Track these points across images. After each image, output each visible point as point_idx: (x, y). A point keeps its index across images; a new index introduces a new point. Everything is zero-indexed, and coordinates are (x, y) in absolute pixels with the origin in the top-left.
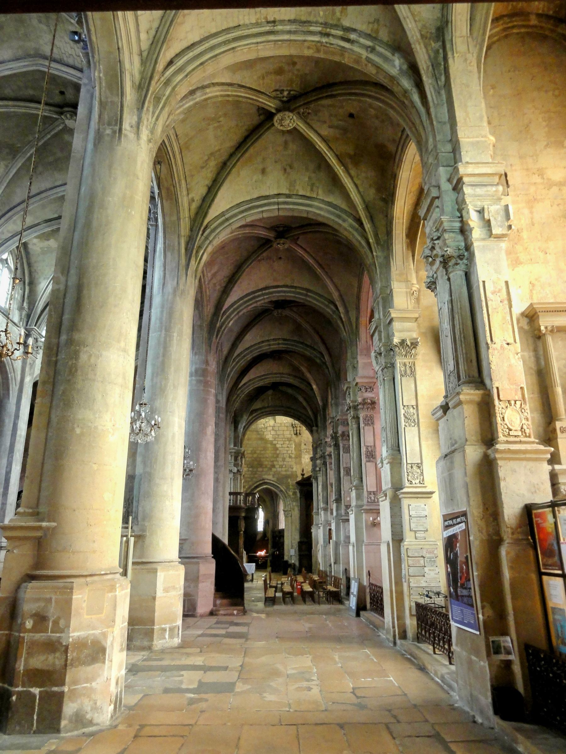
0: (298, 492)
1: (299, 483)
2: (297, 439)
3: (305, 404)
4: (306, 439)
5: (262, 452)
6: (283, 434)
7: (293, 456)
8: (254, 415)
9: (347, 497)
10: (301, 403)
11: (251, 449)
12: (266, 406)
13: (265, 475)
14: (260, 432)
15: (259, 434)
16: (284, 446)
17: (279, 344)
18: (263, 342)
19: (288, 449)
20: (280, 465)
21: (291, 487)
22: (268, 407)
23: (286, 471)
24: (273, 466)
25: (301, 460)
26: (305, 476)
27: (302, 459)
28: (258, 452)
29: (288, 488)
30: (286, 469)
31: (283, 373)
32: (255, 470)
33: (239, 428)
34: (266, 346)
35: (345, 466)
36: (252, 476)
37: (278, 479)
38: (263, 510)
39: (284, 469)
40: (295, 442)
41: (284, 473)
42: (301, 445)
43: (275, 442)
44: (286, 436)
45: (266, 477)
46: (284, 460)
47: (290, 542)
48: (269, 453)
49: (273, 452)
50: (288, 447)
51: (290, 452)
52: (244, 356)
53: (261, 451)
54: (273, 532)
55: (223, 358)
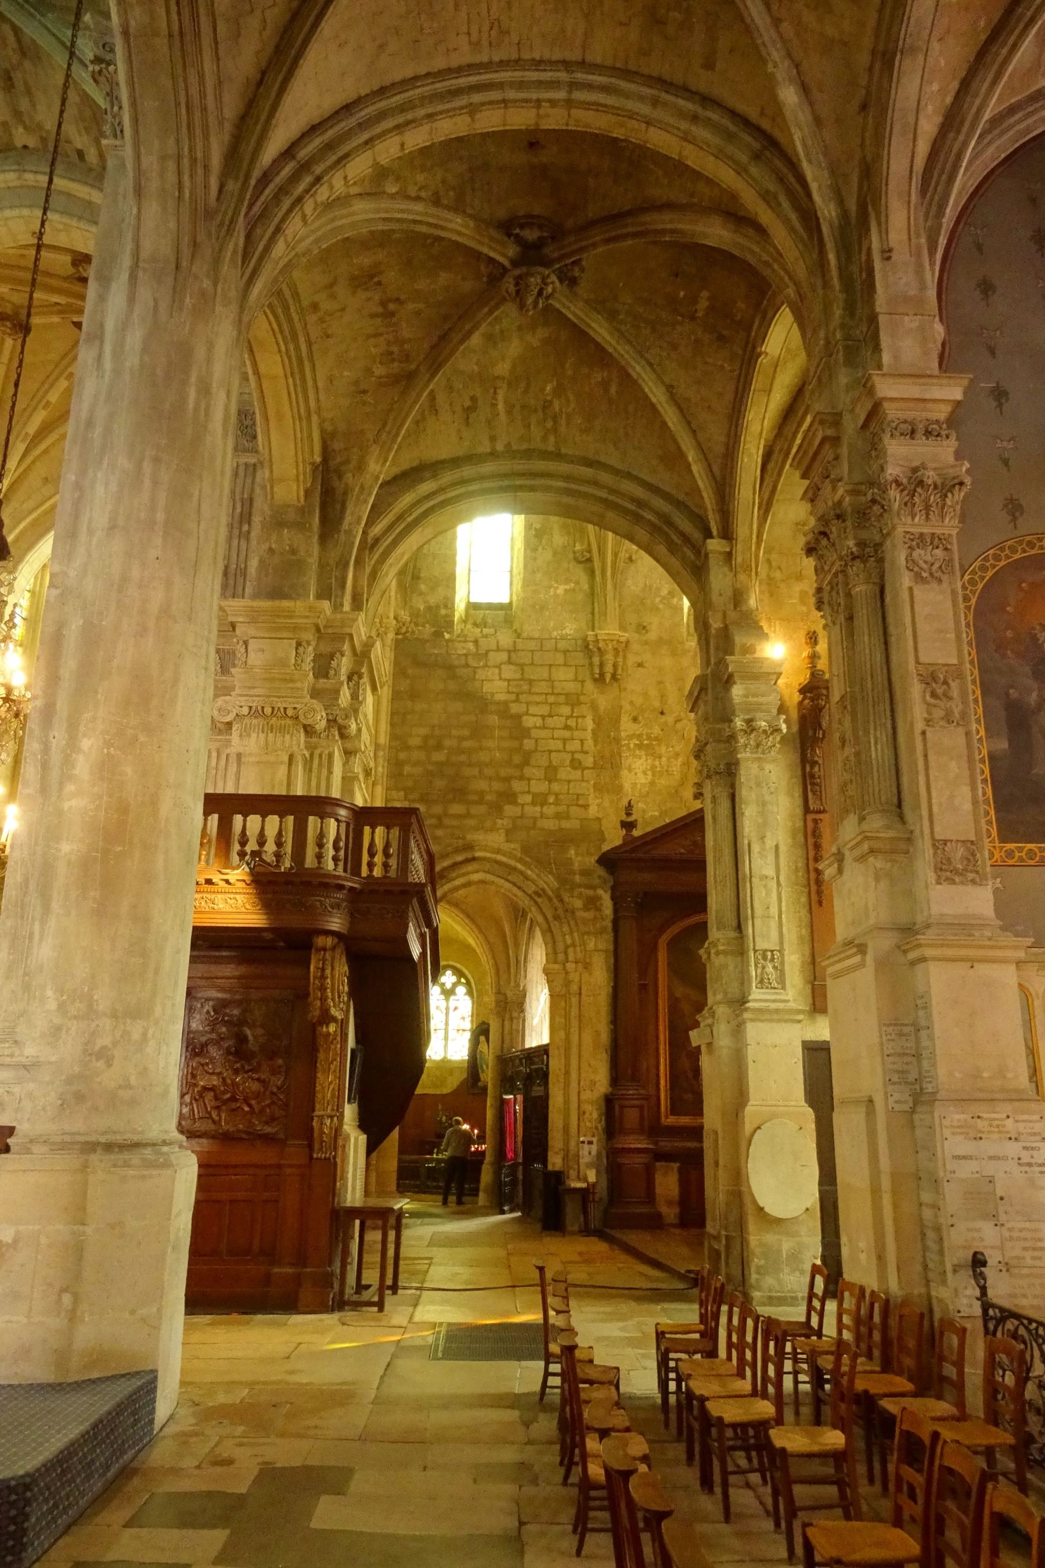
1: (609, 861)
2: (604, 702)
3: (671, 416)
4: (639, 701)
6: (550, 680)
7: (589, 761)
8: (426, 487)
11: (423, 731)
12: (485, 448)
13: (476, 829)
14: (462, 672)
15: (454, 677)
16: (550, 722)
19: (567, 734)
20: (535, 795)
21: (577, 878)
22: (493, 455)
23: (558, 816)
24: (510, 797)
25: (617, 776)
26: (636, 833)
27: (624, 773)
30: (560, 809)
31: (583, 65)
33: (348, 519)
38: (470, 993)
40: (594, 707)
41: (551, 825)
42: (618, 720)
43: (515, 708)
46: (551, 773)
47: (574, 1098)
50: (567, 727)
51: (575, 746)
53: (462, 739)
54: (503, 1061)
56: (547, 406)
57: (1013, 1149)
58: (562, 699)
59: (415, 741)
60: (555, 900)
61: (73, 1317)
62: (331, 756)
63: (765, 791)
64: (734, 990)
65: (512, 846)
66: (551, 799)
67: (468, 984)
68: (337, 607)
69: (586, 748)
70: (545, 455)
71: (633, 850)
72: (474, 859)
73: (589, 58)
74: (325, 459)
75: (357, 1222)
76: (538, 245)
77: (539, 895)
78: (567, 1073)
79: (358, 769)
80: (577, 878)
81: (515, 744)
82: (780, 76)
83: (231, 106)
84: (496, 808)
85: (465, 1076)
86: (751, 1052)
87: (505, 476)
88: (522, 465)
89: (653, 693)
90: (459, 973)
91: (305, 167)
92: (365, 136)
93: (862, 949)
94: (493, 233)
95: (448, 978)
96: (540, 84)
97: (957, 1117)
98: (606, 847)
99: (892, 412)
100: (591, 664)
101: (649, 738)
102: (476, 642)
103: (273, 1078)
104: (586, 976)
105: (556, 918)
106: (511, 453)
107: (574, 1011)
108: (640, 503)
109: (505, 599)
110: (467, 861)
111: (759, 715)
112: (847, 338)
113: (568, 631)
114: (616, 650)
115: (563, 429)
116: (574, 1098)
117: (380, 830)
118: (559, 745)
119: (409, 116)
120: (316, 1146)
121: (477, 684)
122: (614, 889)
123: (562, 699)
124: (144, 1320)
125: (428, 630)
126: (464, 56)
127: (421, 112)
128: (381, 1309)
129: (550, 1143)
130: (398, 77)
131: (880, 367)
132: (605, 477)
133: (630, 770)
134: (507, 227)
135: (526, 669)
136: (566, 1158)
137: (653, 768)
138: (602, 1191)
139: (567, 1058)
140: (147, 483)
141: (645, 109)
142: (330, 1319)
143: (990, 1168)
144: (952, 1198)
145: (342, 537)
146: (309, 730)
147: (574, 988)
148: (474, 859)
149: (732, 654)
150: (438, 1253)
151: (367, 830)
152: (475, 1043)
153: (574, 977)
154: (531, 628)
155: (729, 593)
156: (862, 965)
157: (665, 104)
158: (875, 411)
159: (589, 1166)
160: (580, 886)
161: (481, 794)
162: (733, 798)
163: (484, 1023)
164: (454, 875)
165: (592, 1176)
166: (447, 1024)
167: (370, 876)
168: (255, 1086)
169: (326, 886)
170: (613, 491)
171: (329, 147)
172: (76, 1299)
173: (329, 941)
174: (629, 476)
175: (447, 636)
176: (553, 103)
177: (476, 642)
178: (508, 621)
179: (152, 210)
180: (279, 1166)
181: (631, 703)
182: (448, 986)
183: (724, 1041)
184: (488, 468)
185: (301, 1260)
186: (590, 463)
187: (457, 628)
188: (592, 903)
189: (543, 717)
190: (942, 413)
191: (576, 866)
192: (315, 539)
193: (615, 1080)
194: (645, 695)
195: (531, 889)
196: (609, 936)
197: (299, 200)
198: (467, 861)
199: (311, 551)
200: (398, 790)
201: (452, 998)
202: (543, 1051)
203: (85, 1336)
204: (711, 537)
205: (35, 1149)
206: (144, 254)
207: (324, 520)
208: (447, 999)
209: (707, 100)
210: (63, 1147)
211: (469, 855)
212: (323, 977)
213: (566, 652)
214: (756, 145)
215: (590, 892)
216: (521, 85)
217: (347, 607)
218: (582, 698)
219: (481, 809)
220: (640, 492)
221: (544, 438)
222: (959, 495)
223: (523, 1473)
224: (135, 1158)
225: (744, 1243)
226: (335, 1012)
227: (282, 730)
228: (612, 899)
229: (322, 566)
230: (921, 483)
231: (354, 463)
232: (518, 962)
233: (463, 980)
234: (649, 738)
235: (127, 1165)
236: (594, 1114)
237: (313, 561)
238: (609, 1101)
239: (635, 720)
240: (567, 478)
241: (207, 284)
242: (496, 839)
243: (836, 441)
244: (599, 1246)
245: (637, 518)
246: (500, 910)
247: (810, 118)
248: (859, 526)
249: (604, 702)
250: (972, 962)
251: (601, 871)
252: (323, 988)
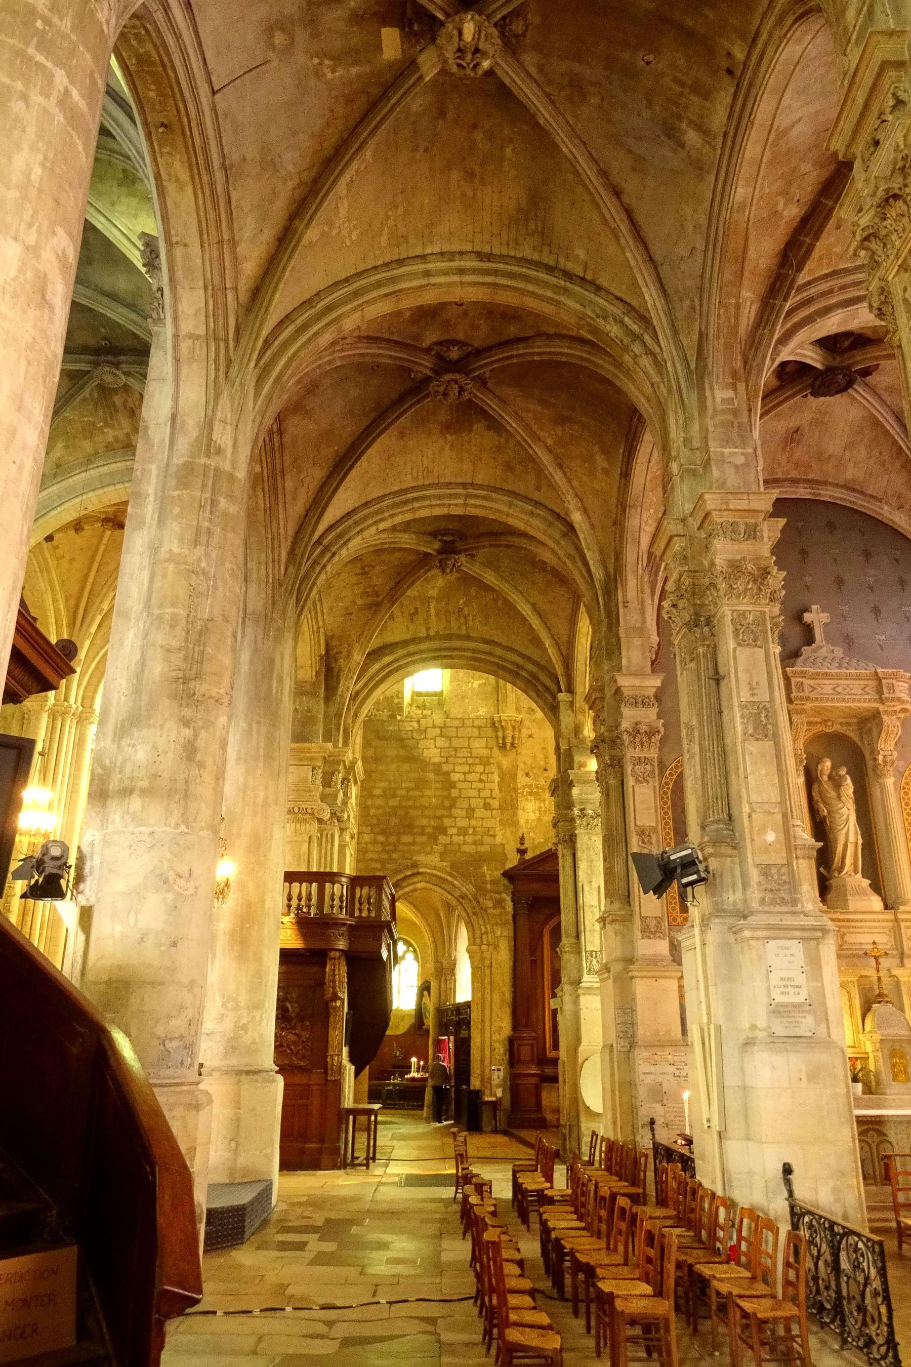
0: (508, 899)
1: (509, 875)
2: (506, 763)
3: (535, 622)
4: (529, 761)
5: (413, 793)
7: (496, 804)
8: (387, 659)
9: (763, 830)
10: (524, 620)
11: (382, 785)
12: (423, 633)
13: (419, 852)
14: (408, 742)
15: (404, 747)
16: (469, 777)
17: (461, 271)
18: (401, 262)
19: (480, 785)
20: (459, 829)
21: (489, 886)
22: (428, 637)
23: (475, 843)
25: (515, 814)
26: (529, 856)
27: (520, 812)
28: (402, 792)
29: (480, 889)
30: (478, 837)
32: (393, 839)
33: (341, 688)
34: (411, 276)
35: (745, 696)
36: (385, 856)
37: (452, 867)
38: (416, 958)
39: (469, 839)
40: (499, 767)
42: (516, 775)
43: (445, 768)
44: (475, 752)
45: (421, 858)
46: (470, 812)
47: (487, 1039)
48: (431, 796)
49: (439, 793)
50: (481, 781)
51: (487, 793)
52: (329, 309)
55: (245, 284)
56: (460, 610)
57: (672, 1069)
58: (477, 761)
59: (378, 792)
61: (236, 1152)
62: (333, 836)
63: (592, 853)
64: (574, 975)
66: (471, 831)
67: (415, 951)
68: (335, 745)
69: (494, 795)
70: (460, 637)
71: (526, 868)
72: (418, 873)
73: (476, 481)
74: (327, 651)
75: (351, 1117)
76: (453, 542)
78: (483, 1021)
79: (348, 838)
80: (489, 886)
81: (446, 793)
82: (571, 507)
83: (291, 529)
84: (434, 838)
85: (413, 1021)
86: (583, 1014)
87: (435, 650)
88: (447, 644)
89: (540, 756)
90: (408, 944)
91: (327, 548)
92: (358, 528)
93: (608, 971)
94: (427, 538)
96: (450, 496)
97: (646, 1054)
98: (509, 865)
99: (626, 692)
100: (497, 737)
101: (537, 788)
102: (418, 721)
103: (304, 1033)
105: (475, 914)
106: (438, 636)
107: (487, 980)
108: (519, 666)
109: (439, 690)
110: (413, 875)
111: (590, 806)
112: (607, 644)
113: (480, 713)
114: (514, 727)
115: (471, 623)
116: (487, 1039)
117: (365, 890)
118: (476, 793)
119: (381, 516)
120: (329, 1072)
121: (420, 751)
122: (513, 893)
123: (477, 761)
124: (266, 1155)
125: (386, 713)
126: (409, 482)
127: (386, 514)
128: (368, 1168)
130: (375, 496)
131: (619, 669)
132: (498, 651)
133: (524, 809)
134: (434, 534)
135: (454, 740)
136: (482, 1081)
137: (540, 808)
138: (507, 1103)
139: (483, 1011)
140: (255, 733)
141: (506, 509)
142: (342, 1172)
143: (660, 1079)
144: (642, 1092)
145: (338, 699)
146: (320, 821)
147: (487, 963)
148: (418, 873)
149: (572, 768)
150: (396, 1143)
151: (358, 890)
152: (420, 996)
153: (487, 955)
154: (456, 711)
155: (572, 726)
156: (609, 978)
157: (516, 506)
158: (618, 691)
159: (498, 1086)
161: (423, 828)
162: (574, 855)
163: (426, 982)
164: (405, 884)
165: (499, 1093)
167: (360, 917)
168: (292, 1038)
169: (336, 924)
170: (500, 658)
171: (340, 536)
172: (237, 1145)
173: (337, 954)
174: (511, 649)
175: (399, 718)
176: (456, 505)
177: (418, 721)
178: (441, 704)
179: (253, 588)
180: (308, 1085)
181: (525, 763)
183: (568, 1007)
184: (424, 646)
185: (322, 1141)
186: (486, 642)
187: (406, 709)
188: (499, 903)
189: (465, 773)
190: (651, 692)
191: (488, 878)
192: (322, 702)
193: (515, 1026)
194: (535, 757)
195: (457, 894)
196: (511, 926)
197: (324, 567)
198: (413, 875)
199: (319, 708)
200: (367, 826)
202: (467, 1005)
203: (242, 1161)
204: (560, 691)
205: (214, 1074)
206: (250, 609)
207: (326, 689)
209: (537, 504)
210: (226, 1073)
211: (415, 871)
212: (334, 975)
213: (480, 728)
214: (563, 529)
216: (440, 497)
217: (340, 745)
218: (491, 760)
219: (424, 839)
220: (519, 660)
221: (460, 628)
222: (658, 737)
223: (443, 1221)
224: (259, 1077)
225: (579, 1127)
226: (340, 994)
227: (305, 821)
228: (513, 900)
229: (325, 716)
230: (638, 732)
231: (344, 654)
232: (450, 939)
234: (537, 788)
235: (257, 1081)
236: (501, 1050)
237: (321, 716)
238: (511, 1040)
239: (527, 775)
240: (474, 651)
241: (280, 622)
242: (434, 860)
243: (602, 699)
244: (503, 1139)
245: (517, 675)
246: (438, 904)
247: (588, 526)
248: (612, 748)
249: (506, 763)
250: (656, 978)
251: (505, 882)
252: (334, 981)
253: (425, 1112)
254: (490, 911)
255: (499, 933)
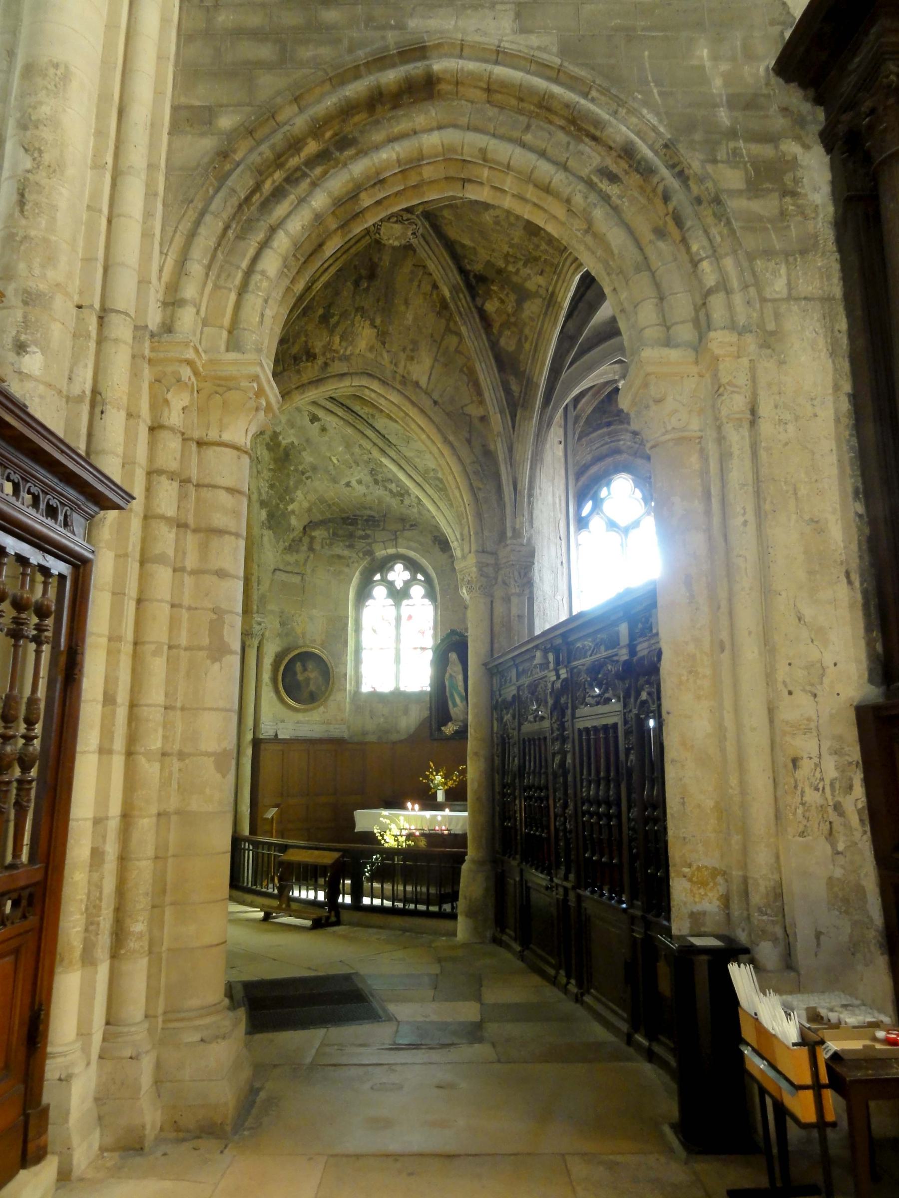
21: (724, 117)
37: (564, 52)
38: (431, 594)
60: (665, 172)
65: (534, 40)
67: (428, 582)
77: (613, 178)
80: (724, 117)
85: (426, 713)
90: (412, 566)
95: (399, 574)
104: (767, 367)
105: (660, 233)
129: (676, 852)
147: (737, 403)
160: (732, 134)
163: (453, 632)
164: (378, 136)
166: (398, 640)
182: (399, 585)
201: (405, 602)
208: (398, 604)
211: (414, 69)
215: (766, 151)
233: (420, 577)
253: (462, 927)
254: (735, 204)
255: (778, 286)
